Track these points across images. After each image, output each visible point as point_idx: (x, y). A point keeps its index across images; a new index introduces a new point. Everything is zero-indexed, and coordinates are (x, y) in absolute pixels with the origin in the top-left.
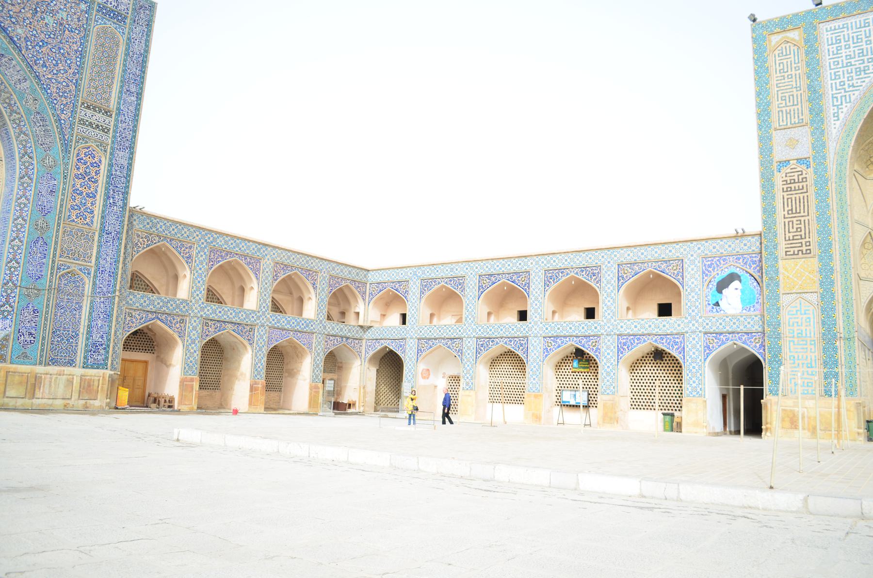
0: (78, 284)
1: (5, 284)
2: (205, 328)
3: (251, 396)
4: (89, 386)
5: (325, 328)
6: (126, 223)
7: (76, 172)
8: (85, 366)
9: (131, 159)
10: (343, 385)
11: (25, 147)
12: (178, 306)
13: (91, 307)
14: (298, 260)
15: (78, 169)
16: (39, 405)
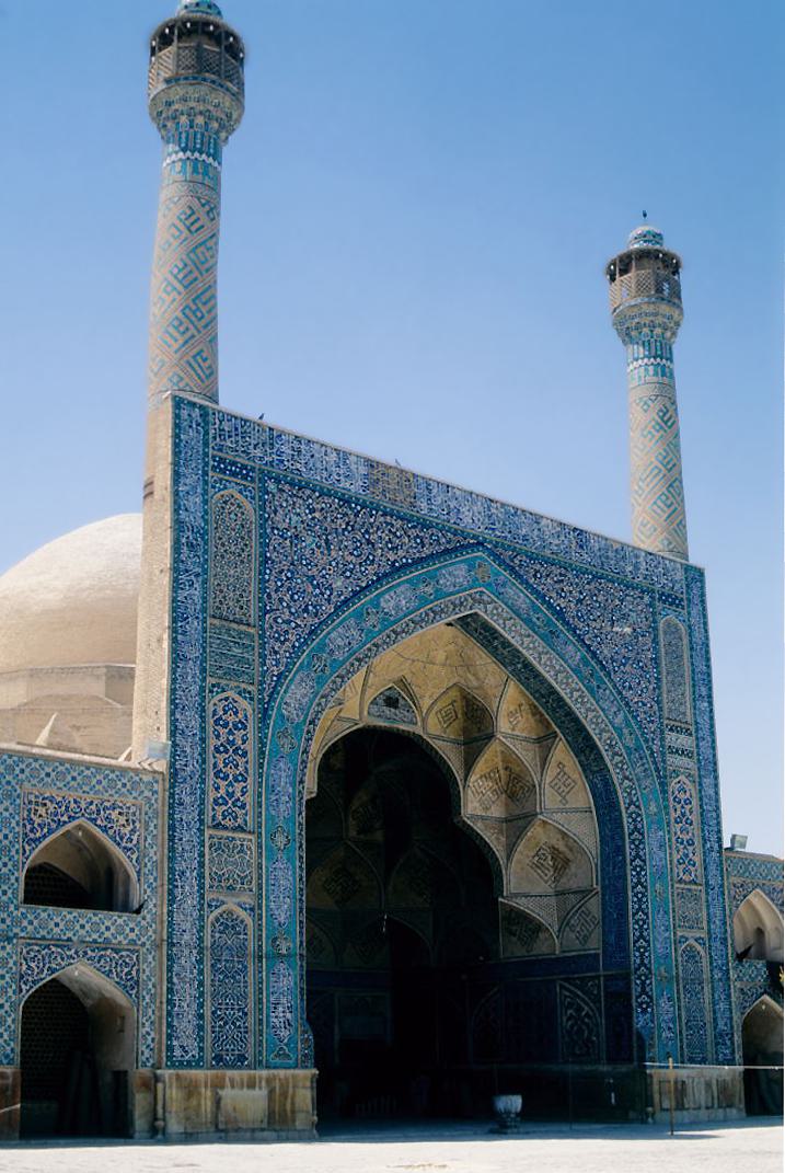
13: (713, 988)
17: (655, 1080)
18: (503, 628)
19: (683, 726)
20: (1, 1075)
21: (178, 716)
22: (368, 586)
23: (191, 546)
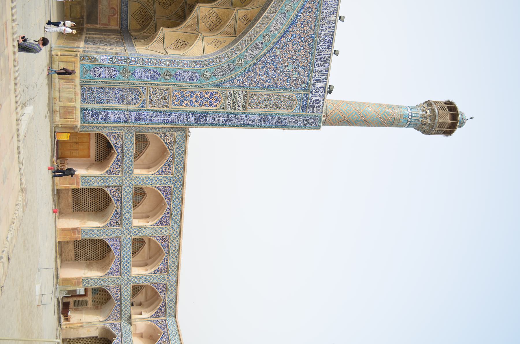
0: (135, 100)
1: (129, 58)
2: (116, 189)
3: (68, 229)
4: (69, 113)
5: (126, 284)
6: (178, 126)
7: (204, 92)
8: (82, 109)
9: (219, 125)
10: (84, 312)
11: (213, 62)
12: (128, 167)
13: (121, 110)
14: (174, 255)
16: (55, 82)
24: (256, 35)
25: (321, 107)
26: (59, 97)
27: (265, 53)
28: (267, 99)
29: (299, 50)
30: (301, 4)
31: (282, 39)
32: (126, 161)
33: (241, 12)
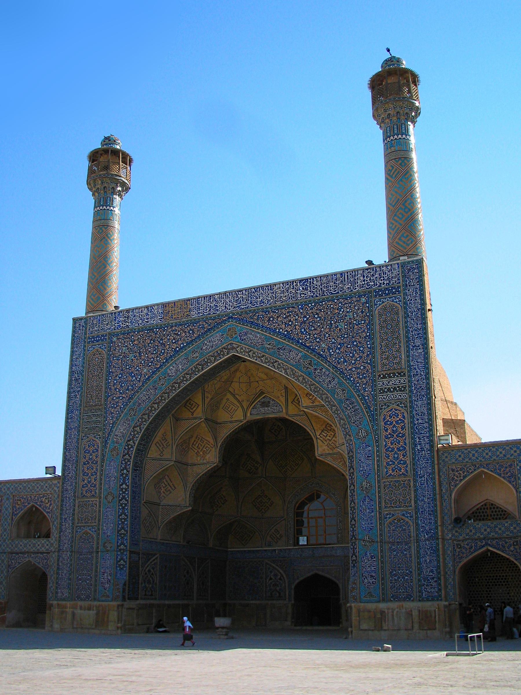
7: (385, 433)
11: (345, 429)
13: (418, 546)
15: (386, 431)
17: (354, 610)
18: (250, 357)
19: (395, 371)
20: (1, 603)
21: (67, 454)
22: (160, 367)
23: (76, 380)
24: (307, 380)
25: (389, 267)
26: (406, 630)
27: (326, 363)
28: (387, 346)
29: (318, 319)
30: (266, 332)
31: (308, 345)
32: (497, 533)
33: (305, 402)
